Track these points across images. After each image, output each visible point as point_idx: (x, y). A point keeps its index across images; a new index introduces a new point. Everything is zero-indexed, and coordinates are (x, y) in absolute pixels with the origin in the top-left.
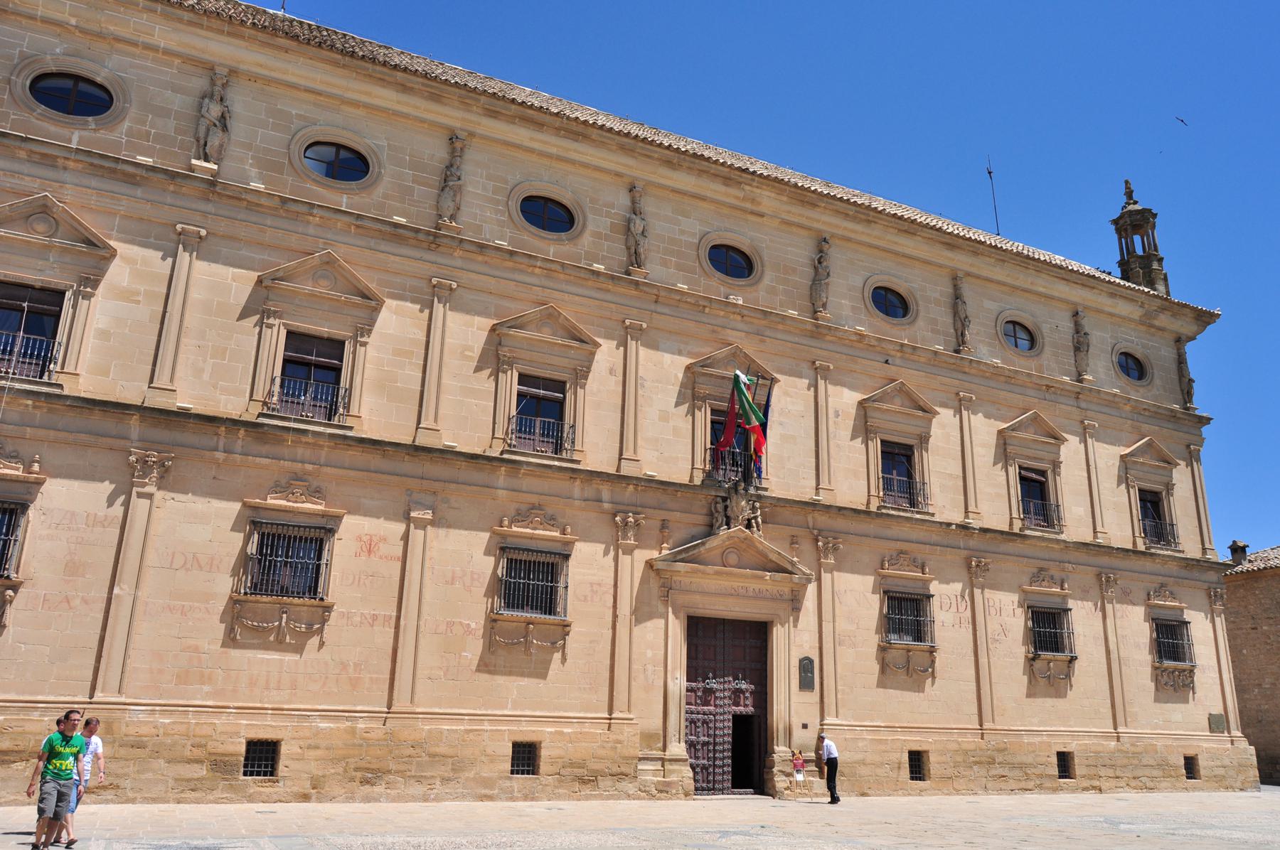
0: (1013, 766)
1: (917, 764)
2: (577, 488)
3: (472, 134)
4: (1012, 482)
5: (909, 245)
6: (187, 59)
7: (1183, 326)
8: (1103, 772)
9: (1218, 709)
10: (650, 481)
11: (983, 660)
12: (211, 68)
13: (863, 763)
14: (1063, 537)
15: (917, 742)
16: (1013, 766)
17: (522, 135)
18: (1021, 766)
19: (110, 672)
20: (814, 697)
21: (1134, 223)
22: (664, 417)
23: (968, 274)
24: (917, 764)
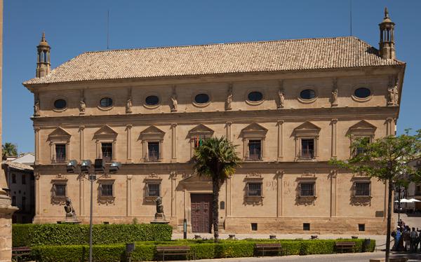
0: (286, 227)
1: (254, 226)
2: (162, 167)
3: (131, 87)
4: (298, 145)
5: (258, 78)
6: (77, 90)
7: (394, 72)
8: (321, 229)
9: (382, 209)
10: (178, 164)
11: (280, 199)
12: (79, 90)
13: (237, 226)
14: (313, 160)
15: (254, 221)
16: (286, 227)
17: (141, 83)
18: (290, 227)
19: (82, 212)
20: (224, 211)
21: (384, 27)
22: (183, 146)
23: (283, 81)
24: (254, 226)
